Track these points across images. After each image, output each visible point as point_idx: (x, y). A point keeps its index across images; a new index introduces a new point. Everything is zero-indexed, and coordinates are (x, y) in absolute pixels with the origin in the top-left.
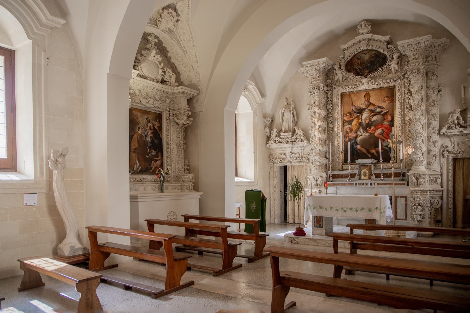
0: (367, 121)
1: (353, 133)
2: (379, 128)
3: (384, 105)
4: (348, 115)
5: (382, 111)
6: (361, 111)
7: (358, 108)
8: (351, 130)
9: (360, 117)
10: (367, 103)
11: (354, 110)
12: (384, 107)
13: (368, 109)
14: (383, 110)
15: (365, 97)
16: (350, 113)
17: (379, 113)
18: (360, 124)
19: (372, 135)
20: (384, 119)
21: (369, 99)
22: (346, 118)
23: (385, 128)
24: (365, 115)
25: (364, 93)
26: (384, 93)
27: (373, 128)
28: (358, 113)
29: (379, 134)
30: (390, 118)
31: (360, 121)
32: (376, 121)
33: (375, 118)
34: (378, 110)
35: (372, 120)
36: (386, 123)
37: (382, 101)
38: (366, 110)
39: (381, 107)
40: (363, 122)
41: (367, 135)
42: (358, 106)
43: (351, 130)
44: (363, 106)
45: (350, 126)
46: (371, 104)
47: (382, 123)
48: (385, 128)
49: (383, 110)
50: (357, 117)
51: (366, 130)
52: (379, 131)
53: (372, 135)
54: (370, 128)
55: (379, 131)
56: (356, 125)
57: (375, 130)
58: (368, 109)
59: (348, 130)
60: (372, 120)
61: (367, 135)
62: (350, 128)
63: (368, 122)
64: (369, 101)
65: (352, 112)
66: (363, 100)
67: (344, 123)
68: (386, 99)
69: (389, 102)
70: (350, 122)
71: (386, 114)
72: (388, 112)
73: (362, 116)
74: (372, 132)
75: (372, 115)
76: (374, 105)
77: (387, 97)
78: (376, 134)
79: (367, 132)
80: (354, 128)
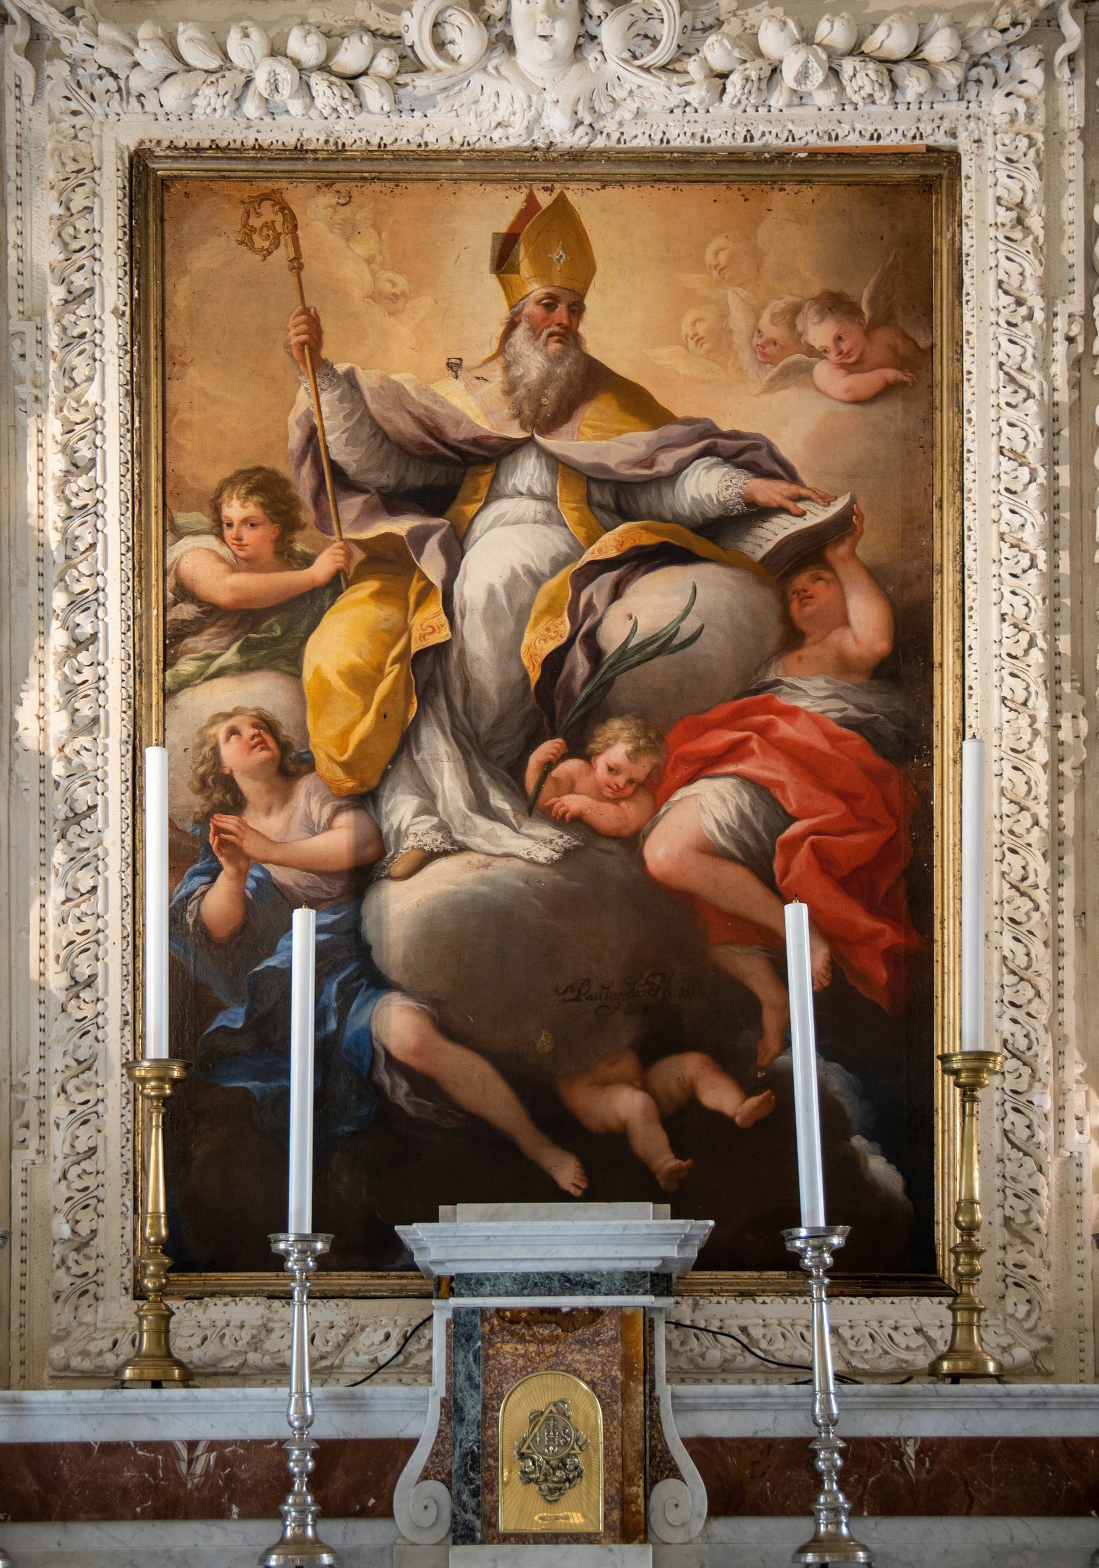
0: (539, 642)
1: (308, 799)
2: (705, 766)
3: (797, 419)
4: (235, 509)
5: (757, 513)
6: (441, 475)
7: (406, 426)
8: (289, 764)
9: (431, 564)
10: (533, 360)
11: (338, 445)
12: (790, 445)
13: (557, 464)
14: (767, 491)
15: (504, 259)
16: (266, 485)
17: (713, 535)
18: (431, 672)
19: (603, 854)
20: (792, 638)
21: (564, 312)
22: (198, 559)
23: (797, 756)
24: (510, 541)
25: (500, 208)
26: (794, 240)
27: (617, 748)
28: (393, 502)
29: (709, 850)
30: (866, 624)
31: (428, 626)
32: (663, 644)
33: (654, 603)
34: (707, 485)
35: (614, 632)
36: (811, 695)
37: (766, 352)
38: (528, 472)
39: (747, 454)
40: (479, 643)
41: (534, 845)
42: (396, 394)
43: (289, 764)
44: (476, 408)
45: (262, 691)
46: (591, 381)
47: (753, 690)
48: (797, 756)
49: (767, 491)
50: (389, 563)
51: (512, 775)
52: (708, 806)
53: (603, 854)
54: (579, 746)
55: (708, 806)
56: (362, 681)
57: (655, 790)
58: (557, 464)
59: (232, 755)
60: (614, 632)
61: (534, 845)
62: (266, 724)
63: (555, 661)
64: (569, 336)
65: (303, 484)
66: (485, 303)
67: (175, 637)
68: (820, 332)
69: (870, 380)
70: (271, 633)
71: (810, 552)
72: (843, 527)
73: (455, 550)
74: (606, 816)
75: (608, 545)
76: (639, 404)
77: (836, 304)
78: (662, 850)
79: (532, 807)
80: (337, 731)
